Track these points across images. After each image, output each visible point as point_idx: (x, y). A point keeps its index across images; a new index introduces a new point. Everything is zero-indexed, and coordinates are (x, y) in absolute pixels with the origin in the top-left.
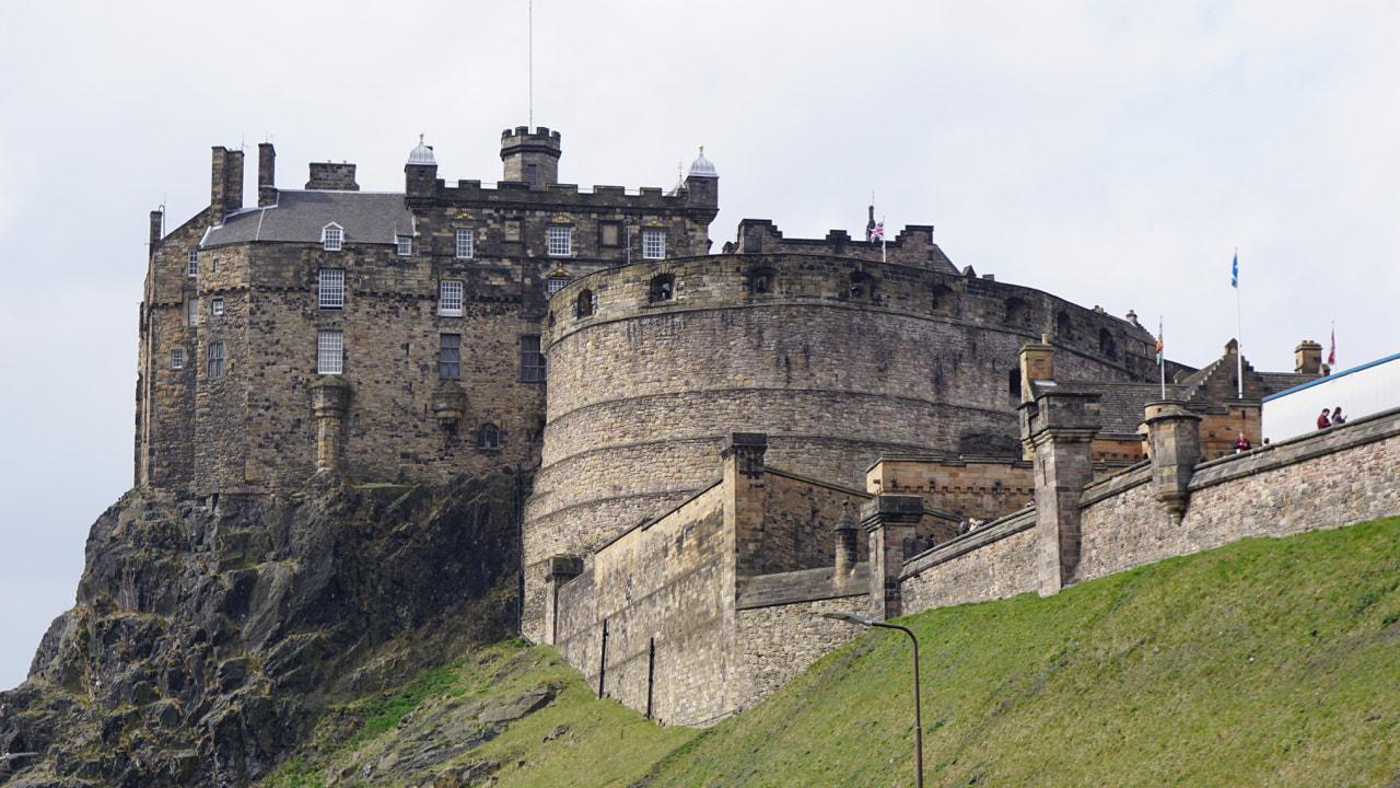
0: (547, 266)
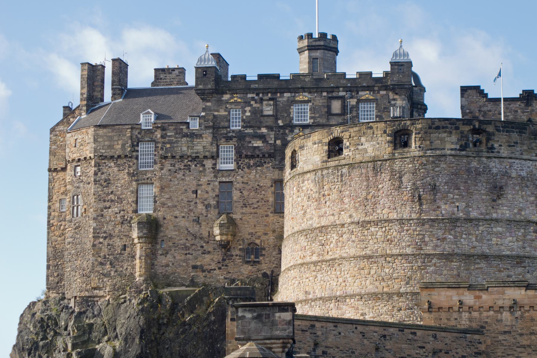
0: (292, 131)
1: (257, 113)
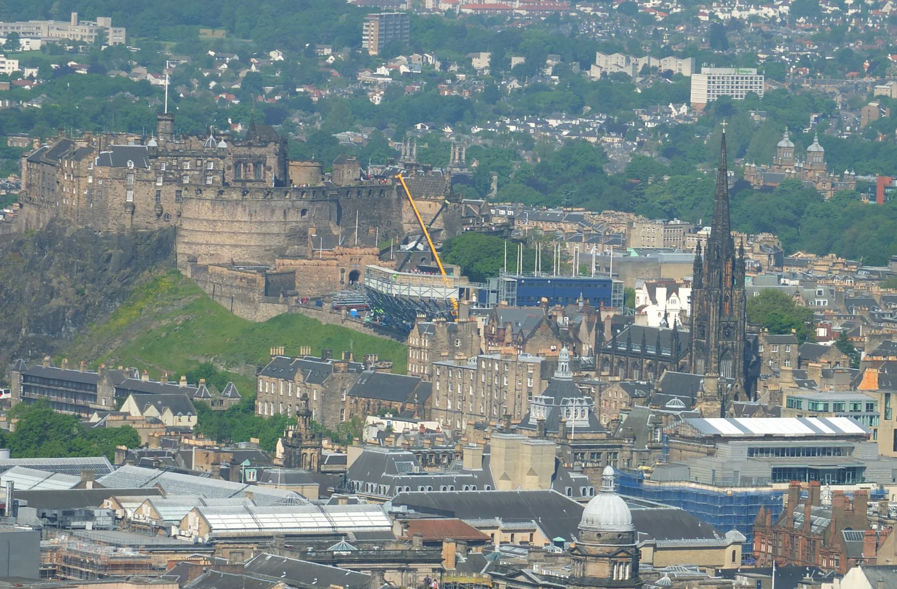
1: (170, 164)
